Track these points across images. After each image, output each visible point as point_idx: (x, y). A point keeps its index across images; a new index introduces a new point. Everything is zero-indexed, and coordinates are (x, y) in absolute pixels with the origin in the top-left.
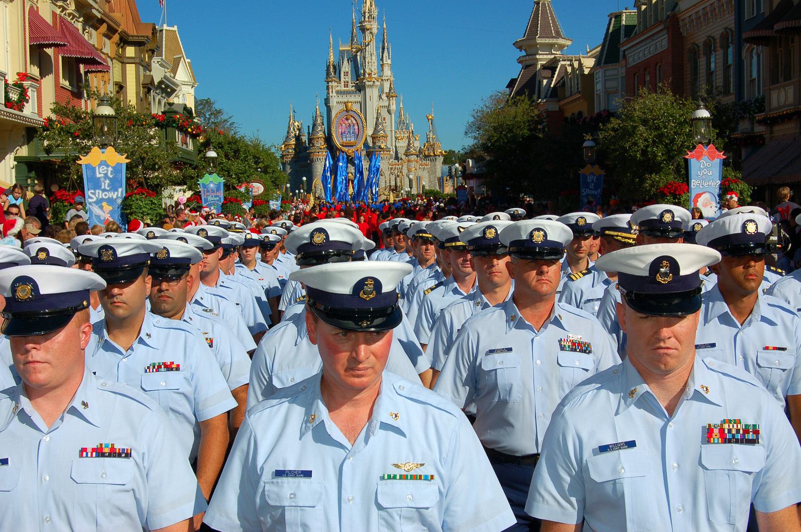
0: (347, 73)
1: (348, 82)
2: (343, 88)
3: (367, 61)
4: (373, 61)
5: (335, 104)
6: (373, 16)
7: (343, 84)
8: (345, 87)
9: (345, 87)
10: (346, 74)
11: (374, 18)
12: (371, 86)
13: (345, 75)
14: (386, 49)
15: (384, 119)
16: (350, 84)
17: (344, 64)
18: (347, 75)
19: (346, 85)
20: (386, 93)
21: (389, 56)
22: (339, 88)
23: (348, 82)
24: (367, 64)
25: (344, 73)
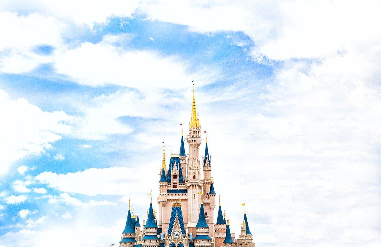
0: (176, 176)
2: (172, 188)
7: (172, 185)
8: (174, 187)
9: (174, 187)
10: (175, 176)
13: (174, 178)
15: (206, 214)
16: (178, 185)
17: (173, 169)
20: (207, 194)
22: (170, 188)
23: (176, 183)
25: (174, 176)
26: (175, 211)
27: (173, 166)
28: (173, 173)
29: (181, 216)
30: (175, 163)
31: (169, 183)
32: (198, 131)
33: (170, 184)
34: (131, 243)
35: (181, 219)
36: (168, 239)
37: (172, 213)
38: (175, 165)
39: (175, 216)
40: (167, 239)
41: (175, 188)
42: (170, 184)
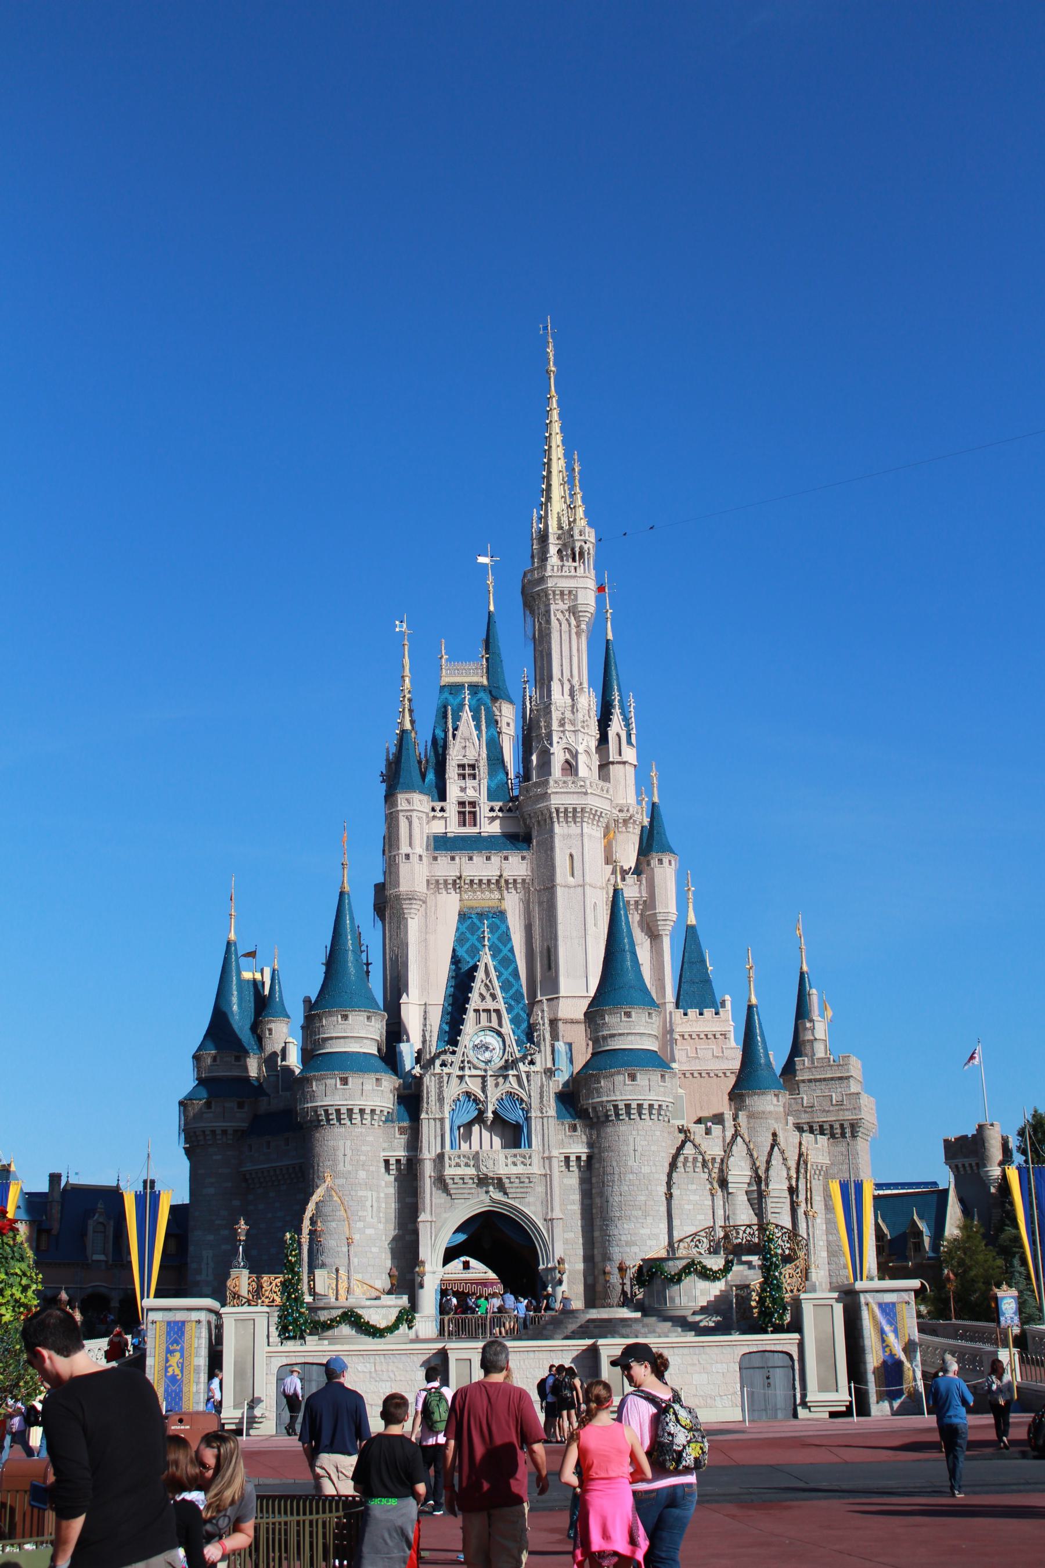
1: (473, 804)
2: (454, 828)
3: (555, 716)
4: (580, 716)
5: (421, 887)
6: (578, 545)
8: (464, 824)
10: (469, 770)
11: (581, 554)
12: (574, 815)
14: (617, 711)
17: (459, 733)
18: (474, 777)
19: (468, 812)
21: (629, 735)
22: (438, 828)
24: (555, 726)
26: (473, 929)
27: (457, 718)
28: (455, 756)
29: (505, 951)
30: (467, 707)
31: (438, 805)
32: (581, 548)
33: (442, 810)
34: (241, 1105)
35: (510, 969)
36: (440, 1075)
37: (460, 940)
38: (467, 715)
39: (474, 951)
40: (439, 1071)
41: (469, 830)
42: (442, 810)
